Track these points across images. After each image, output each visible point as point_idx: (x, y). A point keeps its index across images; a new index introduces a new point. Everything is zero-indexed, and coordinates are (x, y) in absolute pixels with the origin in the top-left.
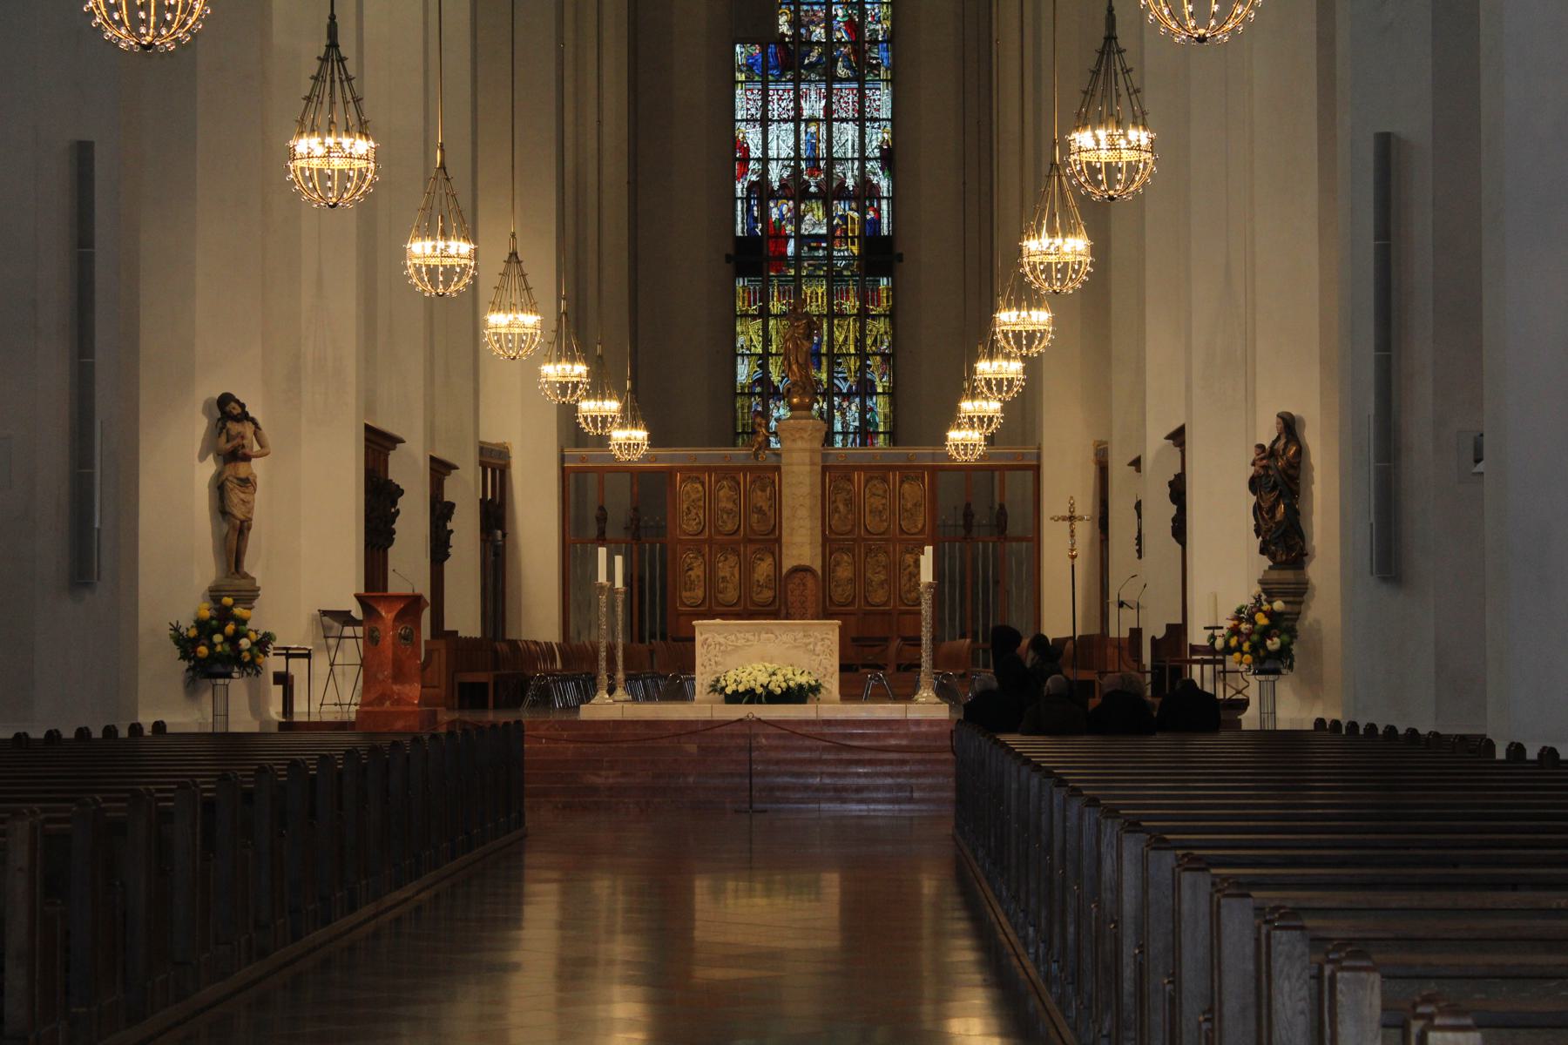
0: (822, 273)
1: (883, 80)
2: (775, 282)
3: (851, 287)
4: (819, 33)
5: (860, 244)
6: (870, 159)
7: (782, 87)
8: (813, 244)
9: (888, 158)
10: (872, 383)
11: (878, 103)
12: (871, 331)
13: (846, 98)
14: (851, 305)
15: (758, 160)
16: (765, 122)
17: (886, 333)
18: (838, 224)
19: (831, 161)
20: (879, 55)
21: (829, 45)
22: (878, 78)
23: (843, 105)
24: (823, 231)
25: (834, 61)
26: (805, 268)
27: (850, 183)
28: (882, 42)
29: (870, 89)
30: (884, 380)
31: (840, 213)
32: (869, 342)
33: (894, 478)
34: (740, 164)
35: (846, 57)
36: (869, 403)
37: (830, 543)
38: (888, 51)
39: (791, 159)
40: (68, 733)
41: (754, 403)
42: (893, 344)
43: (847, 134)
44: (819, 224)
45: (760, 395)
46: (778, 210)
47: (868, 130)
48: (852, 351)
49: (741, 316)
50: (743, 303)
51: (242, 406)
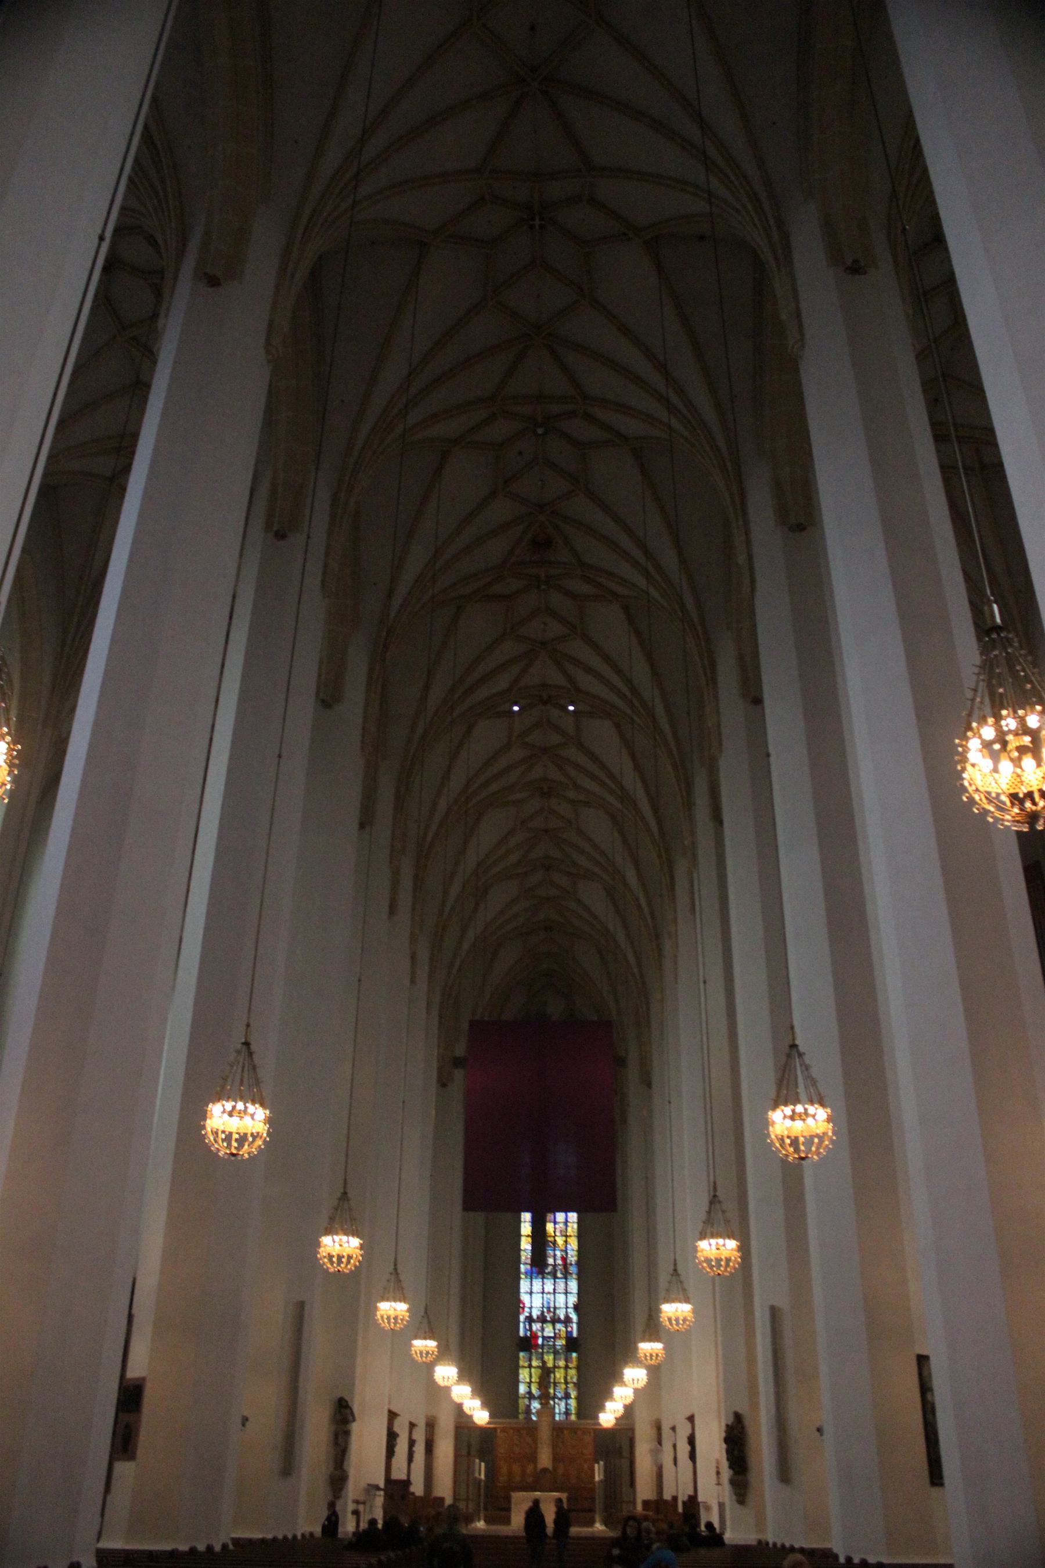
8: (548, 1340)
9: (576, 1308)
10: (570, 1394)
13: (561, 1285)
14: (562, 1363)
19: (555, 1308)
20: (573, 1269)
21: (555, 1266)
24: (552, 1335)
27: (562, 1317)
32: (569, 1378)
35: (561, 1270)
36: (569, 1402)
37: (556, 1459)
40: (280, 1537)
42: (578, 1380)
43: (561, 1299)
45: (528, 1398)
47: (568, 1297)
48: (563, 1381)
51: (347, 1402)
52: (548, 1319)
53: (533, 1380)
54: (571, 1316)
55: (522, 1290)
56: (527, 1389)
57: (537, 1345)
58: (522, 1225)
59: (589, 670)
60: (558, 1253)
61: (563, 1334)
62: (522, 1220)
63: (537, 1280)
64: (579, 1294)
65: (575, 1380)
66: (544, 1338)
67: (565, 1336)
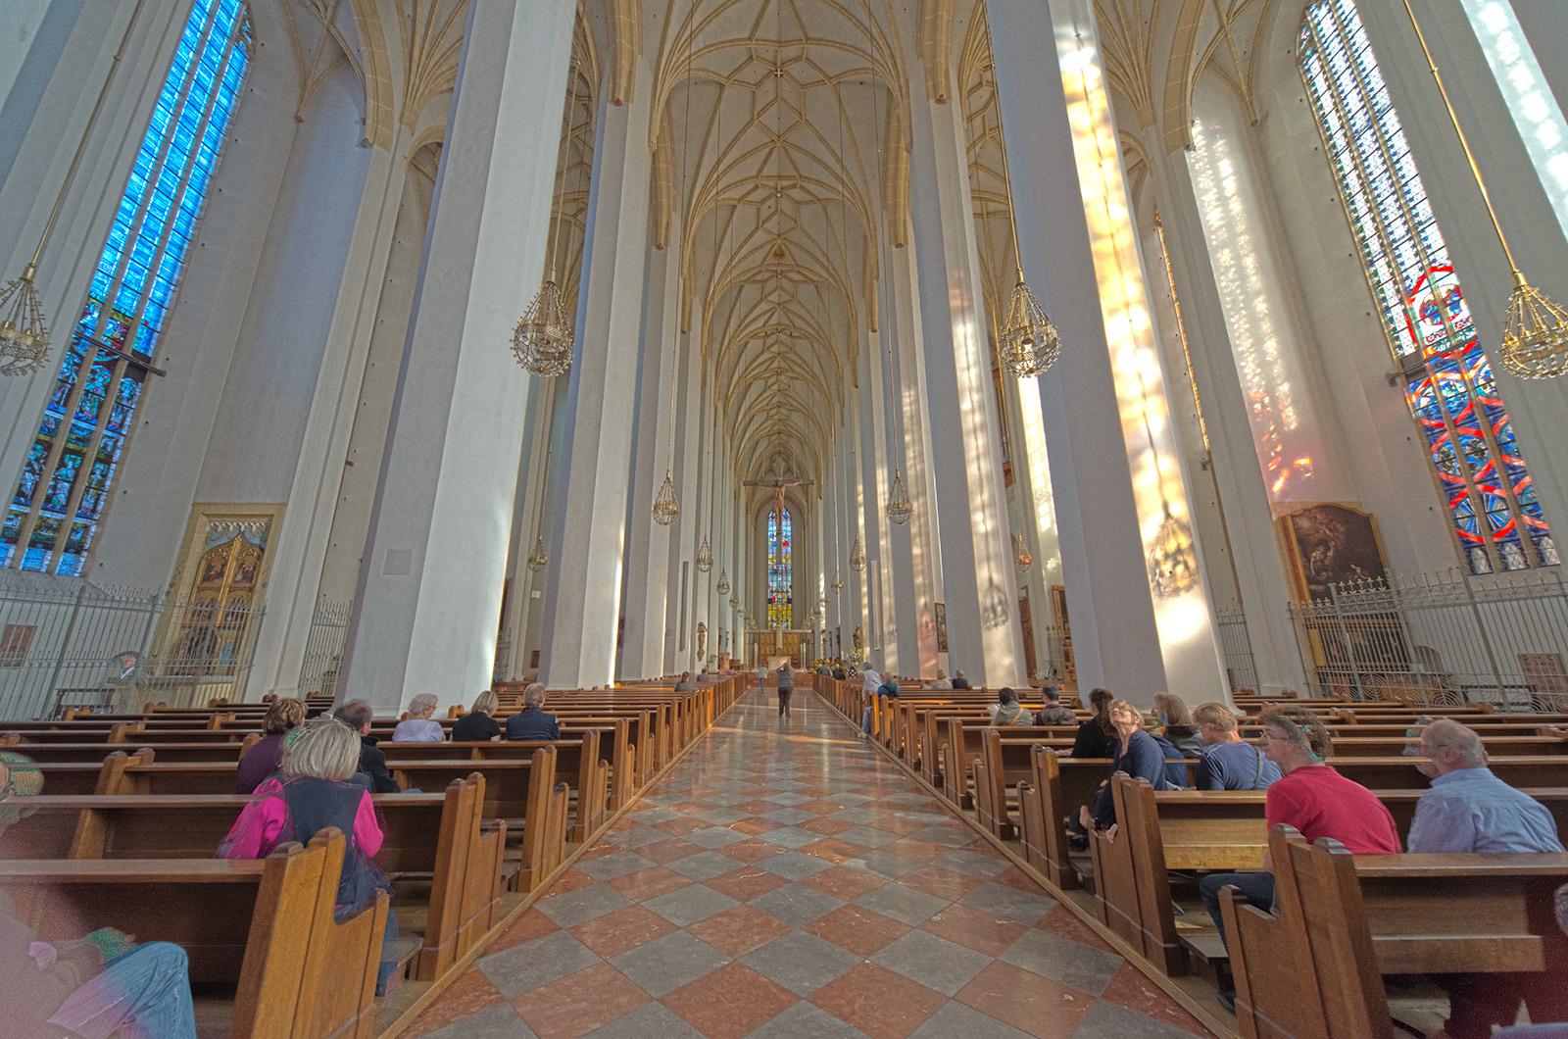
37: (784, 644)
59: (800, 317)
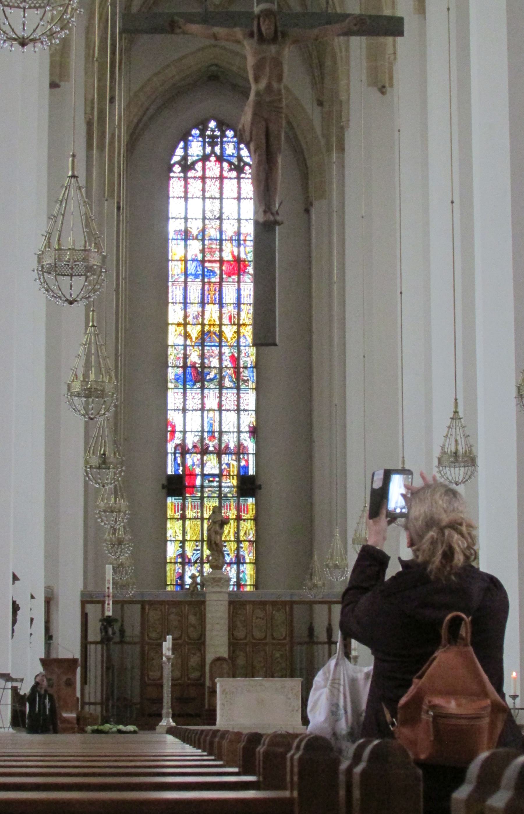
0: (216, 495)
1: (251, 389)
2: (190, 500)
3: (232, 503)
4: (215, 362)
5: (237, 479)
6: (243, 432)
7: (195, 392)
9: (254, 432)
10: (244, 558)
11: (247, 401)
12: (243, 528)
14: (232, 514)
15: (181, 432)
16: (184, 410)
17: (251, 529)
18: (225, 468)
21: (221, 369)
22: (247, 387)
23: (228, 402)
24: (217, 472)
25: (222, 379)
26: (207, 492)
27: (232, 446)
28: (250, 368)
29: (243, 393)
30: (250, 555)
31: (226, 462)
32: (242, 533)
33: (269, 608)
34: (171, 434)
36: (242, 568)
38: (253, 373)
39: (199, 432)
41: (177, 568)
44: (215, 468)
45: (180, 563)
46: (192, 460)
47: (241, 416)
48: (233, 539)
49: (170, 519)
50: (172, 511)
52: (211, 449)
53: (188, 537)
54: (245, 444)
55: (170, 406)
56: (180, 551)
57: (194, 486)
58: (171, 307)
60: (225, 350)
61: (234, 471)
62: (170, 300)
63: (194, 391)
64: (258, 411)
65: (251, 537)
66: (203, 476)
67: (235, 473)
